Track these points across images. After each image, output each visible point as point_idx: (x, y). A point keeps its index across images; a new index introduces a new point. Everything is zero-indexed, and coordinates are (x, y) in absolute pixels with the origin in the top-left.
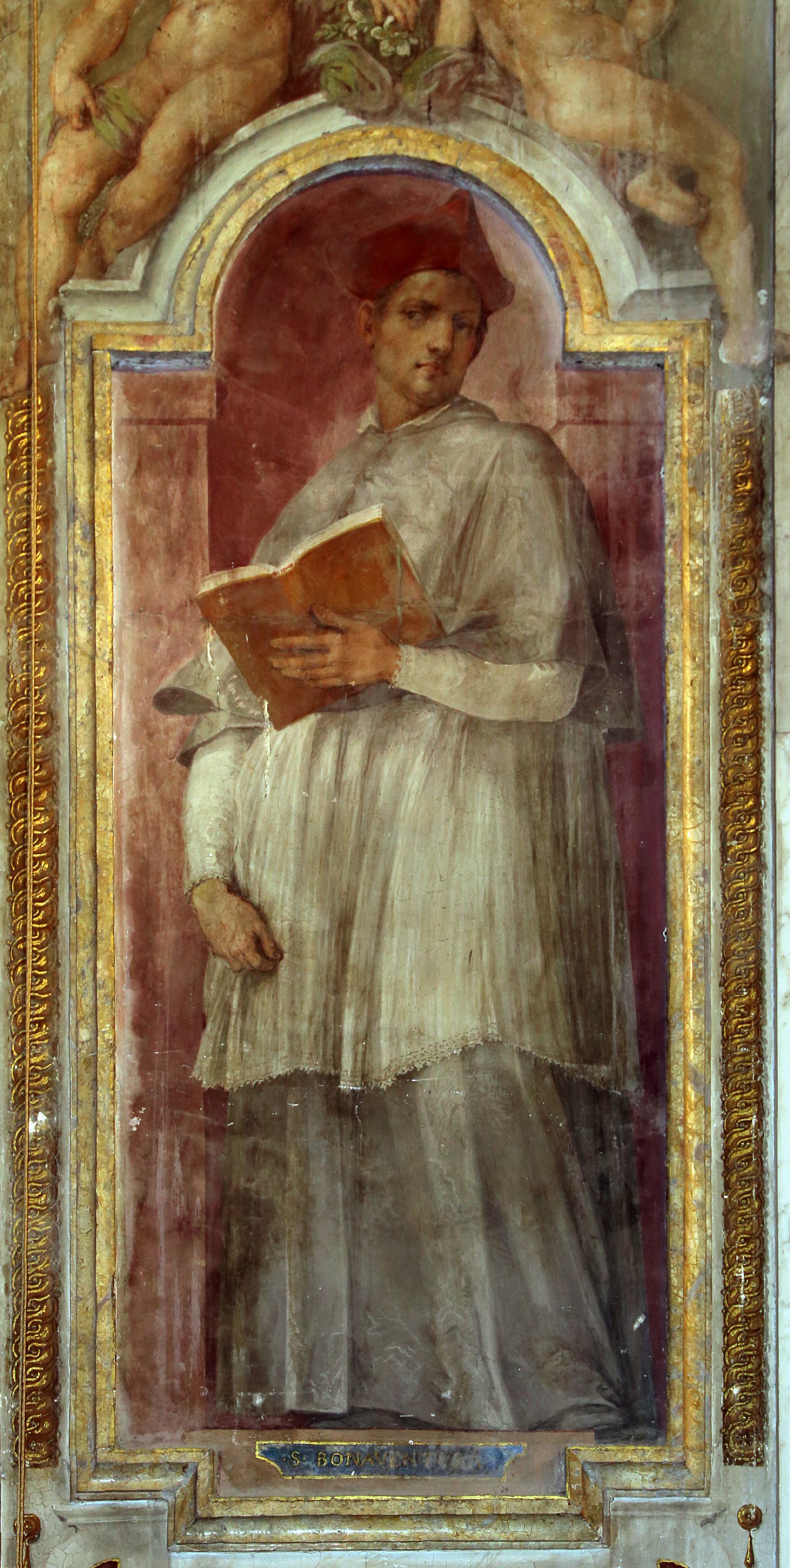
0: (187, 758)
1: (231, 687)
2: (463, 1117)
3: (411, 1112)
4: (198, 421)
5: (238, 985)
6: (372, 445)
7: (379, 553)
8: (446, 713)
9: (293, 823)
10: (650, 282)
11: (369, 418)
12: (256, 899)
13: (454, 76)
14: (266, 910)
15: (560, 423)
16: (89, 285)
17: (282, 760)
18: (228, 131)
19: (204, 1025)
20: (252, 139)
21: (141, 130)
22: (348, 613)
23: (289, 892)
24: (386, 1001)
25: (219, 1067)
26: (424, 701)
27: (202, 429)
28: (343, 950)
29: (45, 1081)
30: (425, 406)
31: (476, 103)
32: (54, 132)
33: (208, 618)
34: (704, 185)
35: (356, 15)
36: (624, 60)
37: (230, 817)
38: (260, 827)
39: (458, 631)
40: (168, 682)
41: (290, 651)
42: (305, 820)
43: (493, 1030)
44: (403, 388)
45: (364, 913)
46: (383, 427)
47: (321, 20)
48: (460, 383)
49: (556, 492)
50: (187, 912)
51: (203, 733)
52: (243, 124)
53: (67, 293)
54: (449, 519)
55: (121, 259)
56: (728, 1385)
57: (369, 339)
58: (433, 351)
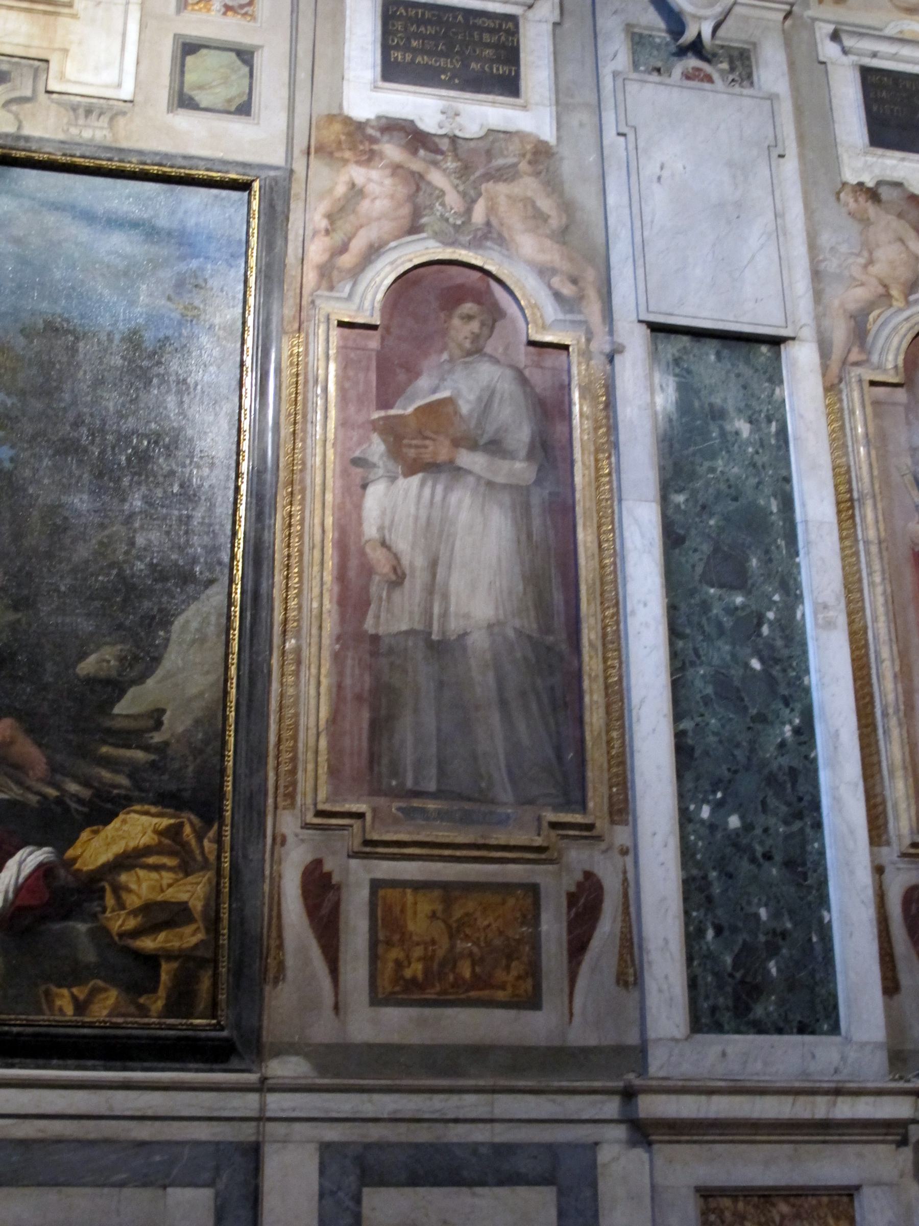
0: (364, 487)
1: (385, 459)
2: (488, 656)
3: (464, 649)
4: (372, 350)
5: (386, 588)
6: (447, 367)
7: (450, 409)
8: (479, 478)
9: (411, 519)
10: (561, 316)
11: (445, 356)
12: (394, 549)
13: (480, 233)
14: (399, 555)
15: (526, 367)
16: (327, 293)
17: (407, 491)
18: (387, 243)
19: (370, 605)
20: (396, 247)
21: (350, 239)
22: (436, 433)
23: (409, 549)
24: (453, 600)
25: (377, 624)
26: (469, 472)
27: (374, 354)
28: (434, 575)
29: (295, 624)
30: (469, 353)
31: (489, 244)
32: (314, 236)
33: (374, 430)
34: (581, 284)
35: (440, 208)
36: (547, 236)
37: (383, 513)
38: (396, 518)
39: (486, 444)
40: (357, 454)
41: (410, 446)
42: (417, 518)
43: (501, 617)
44: (460, 346)
45: (443, 560)
46: (451, 360)
47: (425, 209)
48: (484, 347)
49: (525, 392)
50: (363, 553)
51: (372, 477)
52: (393, 240)
53: (317, 296)
54: (479, 399)
55: (341, 284)
56: (611, 787)
57: (446, 325)
58: (473, 333)
